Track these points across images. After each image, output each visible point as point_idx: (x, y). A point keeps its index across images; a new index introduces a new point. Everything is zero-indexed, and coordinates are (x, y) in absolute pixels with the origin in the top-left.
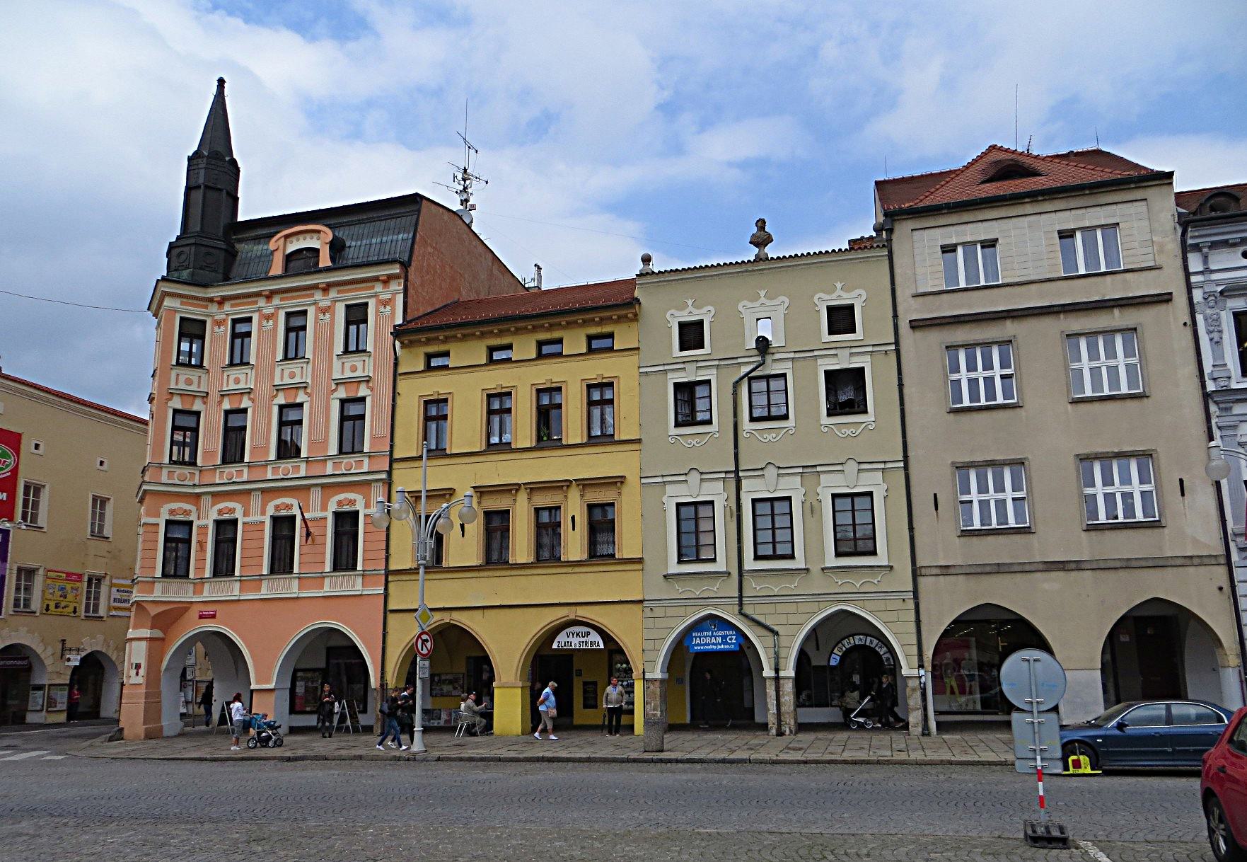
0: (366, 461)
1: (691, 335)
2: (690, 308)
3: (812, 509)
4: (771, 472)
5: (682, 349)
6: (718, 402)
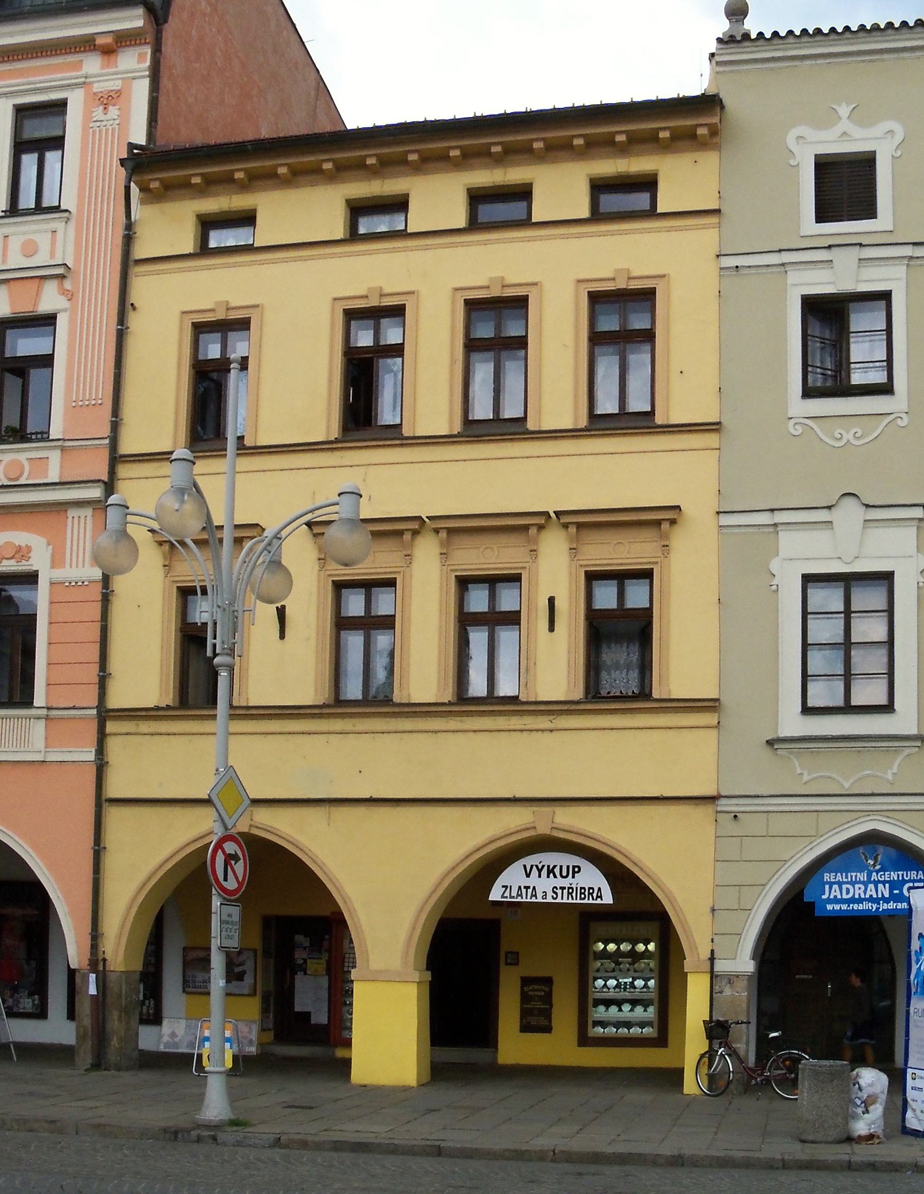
0: (55, 457)
1: (845, 186)
2: (845, 125)
5: (822, 216)
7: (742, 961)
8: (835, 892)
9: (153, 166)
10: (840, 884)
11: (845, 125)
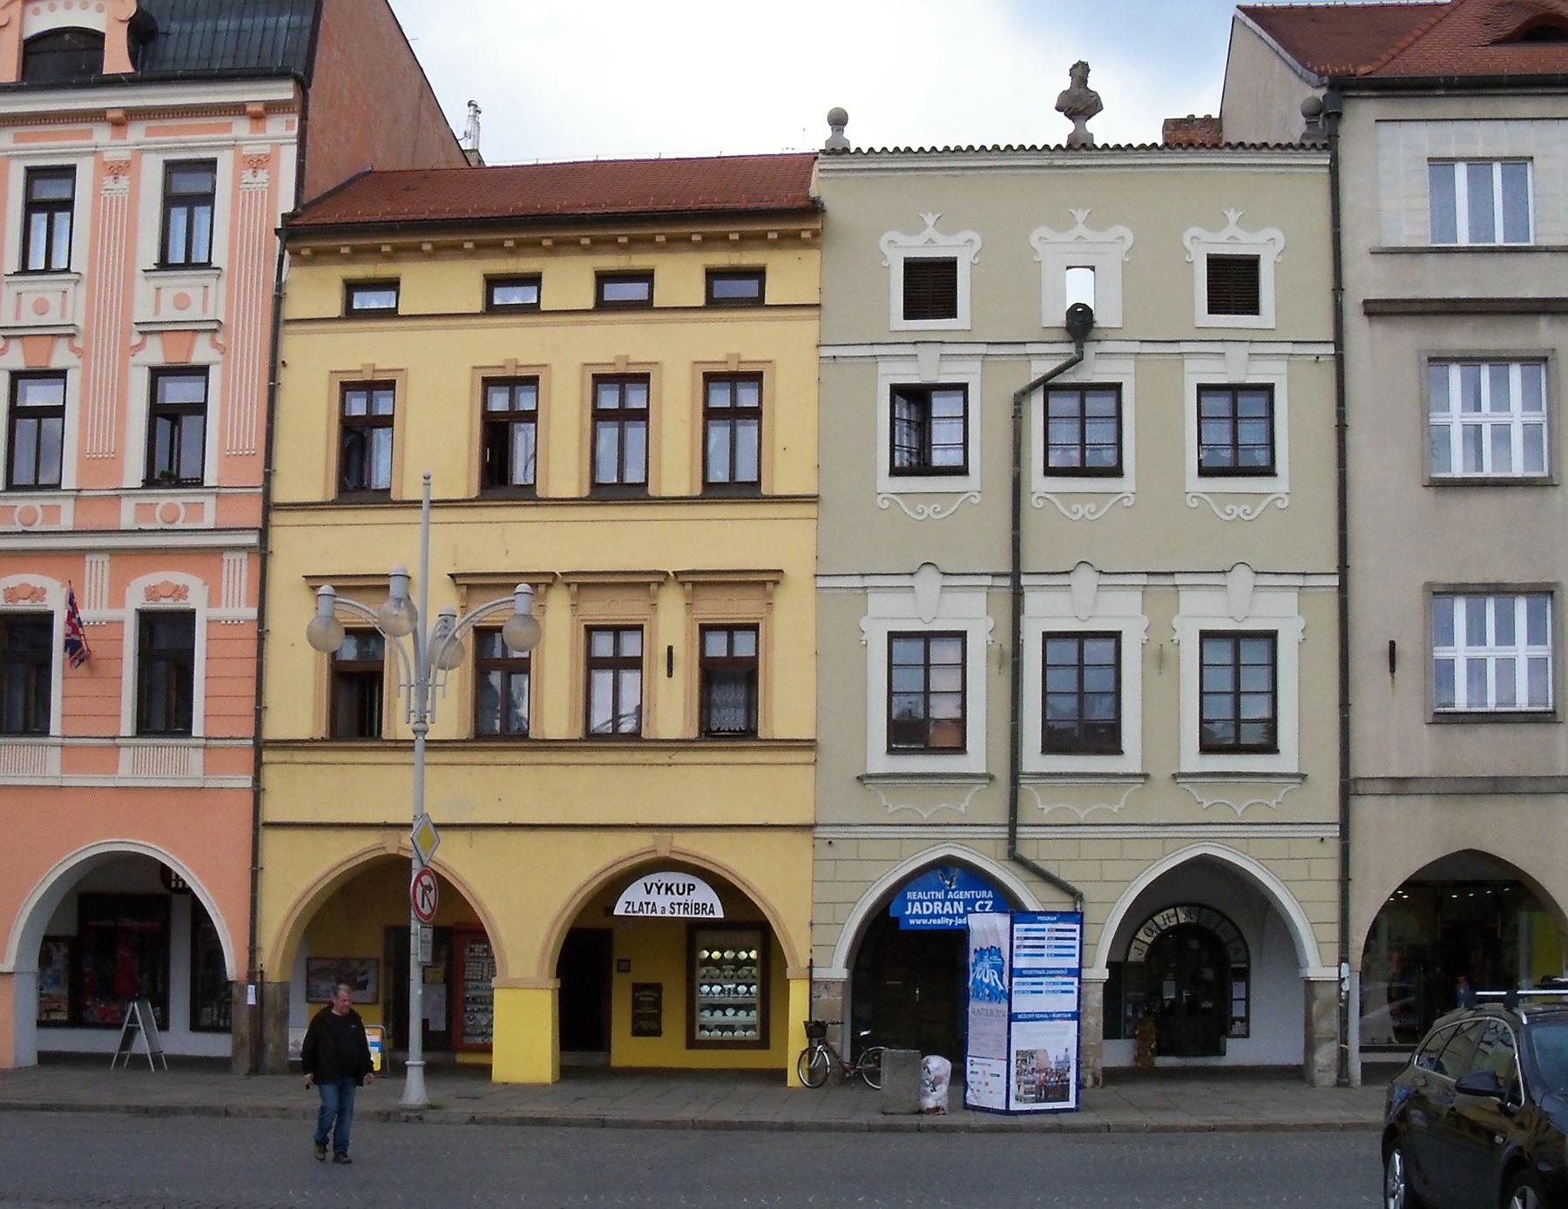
0: (210, 503)
1: (930, 288)
2: (930, 232)
3: (1160, 658)
4: (1085, 580)
5: (908, 315)
6: (976, 431)
7: (837, 969)
8: (917, 909)
9: (303, 234)
10: (921, 901)
11: (930, 232)
